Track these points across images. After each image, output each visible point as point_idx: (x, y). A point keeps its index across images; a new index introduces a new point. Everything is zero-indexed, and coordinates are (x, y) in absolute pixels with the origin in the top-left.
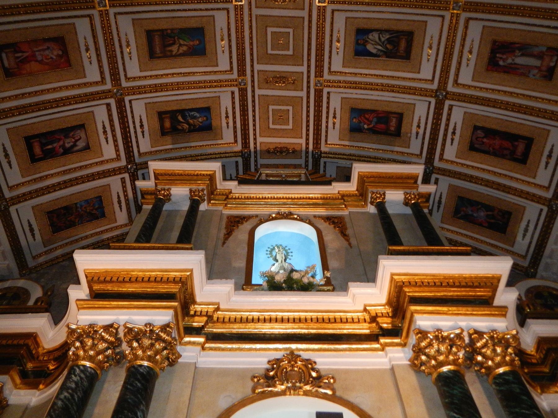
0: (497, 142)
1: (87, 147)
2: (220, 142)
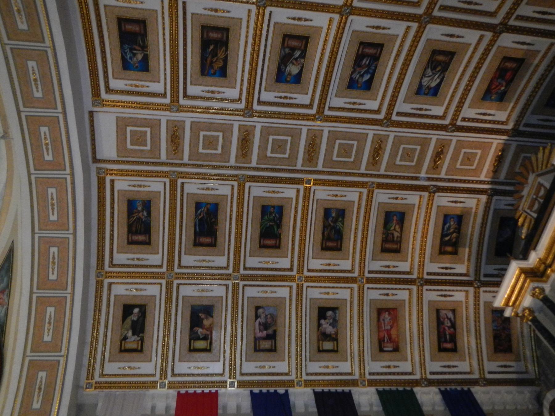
1: (454, 311)
2: (474, 210)
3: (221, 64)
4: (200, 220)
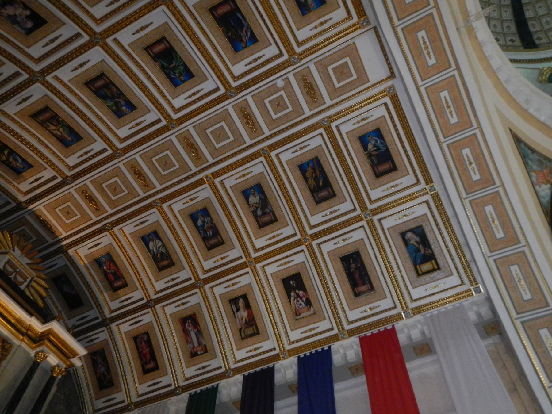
0: (146, 351)
3: (308, 174)
4: (241, 26)
